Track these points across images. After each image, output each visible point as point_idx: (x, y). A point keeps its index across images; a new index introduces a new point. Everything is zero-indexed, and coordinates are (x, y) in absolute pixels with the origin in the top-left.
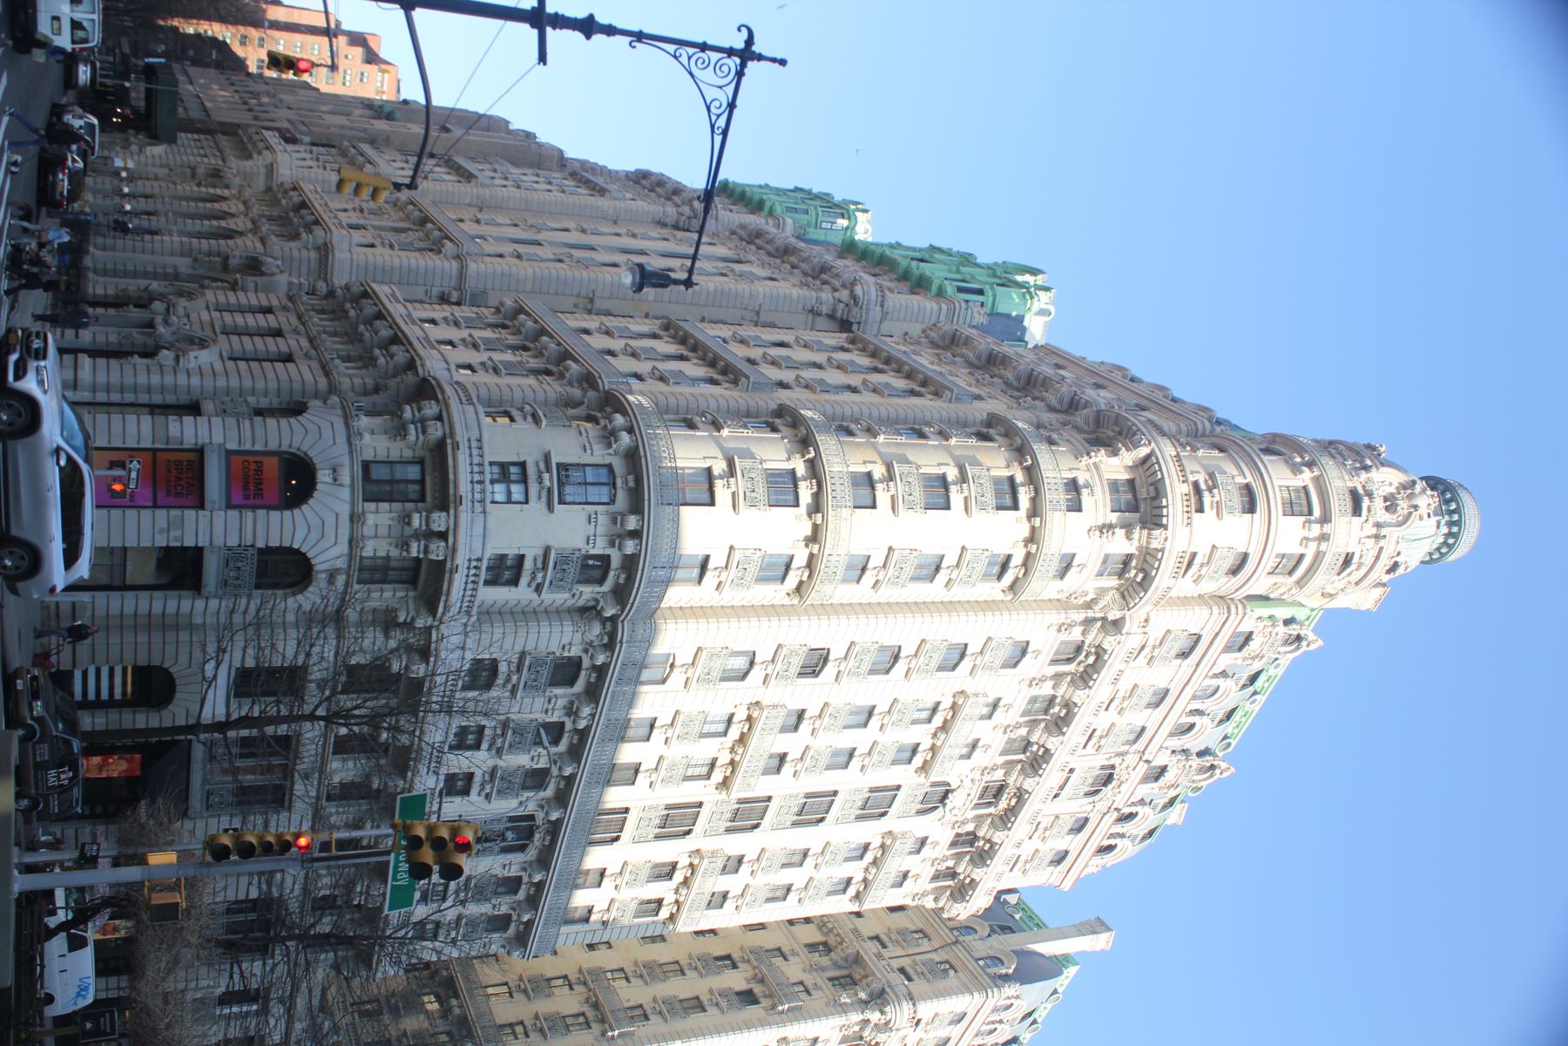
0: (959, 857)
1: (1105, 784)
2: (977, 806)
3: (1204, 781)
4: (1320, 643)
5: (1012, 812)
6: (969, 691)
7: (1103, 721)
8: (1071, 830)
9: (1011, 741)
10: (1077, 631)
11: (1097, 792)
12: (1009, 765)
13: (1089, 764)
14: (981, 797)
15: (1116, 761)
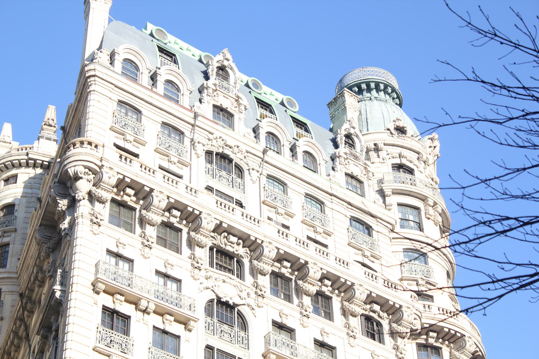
0: (300, 292)
1: (231, 161)
2: (241, 276)
3: (238, 77)
4: (225, 51)
5: (245, 239)
6: (92, 279)
7: (298, 230)
8: (370, 234)
9: (316, 311)
10: (198, 251)
11: (238, 167)
12: (191, 243)
13: (199, 172)
14: (231, 271)
15: (201, 150)
